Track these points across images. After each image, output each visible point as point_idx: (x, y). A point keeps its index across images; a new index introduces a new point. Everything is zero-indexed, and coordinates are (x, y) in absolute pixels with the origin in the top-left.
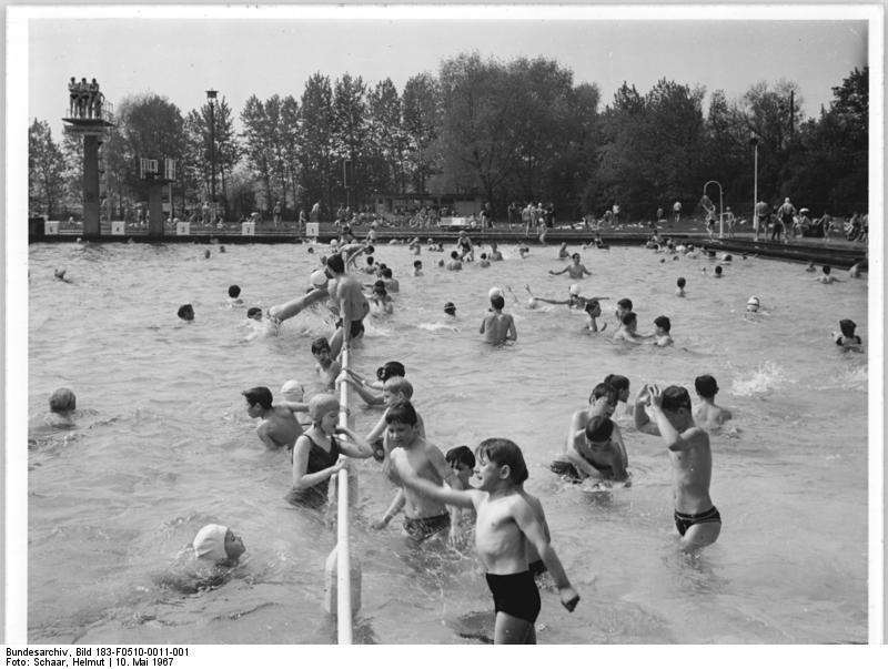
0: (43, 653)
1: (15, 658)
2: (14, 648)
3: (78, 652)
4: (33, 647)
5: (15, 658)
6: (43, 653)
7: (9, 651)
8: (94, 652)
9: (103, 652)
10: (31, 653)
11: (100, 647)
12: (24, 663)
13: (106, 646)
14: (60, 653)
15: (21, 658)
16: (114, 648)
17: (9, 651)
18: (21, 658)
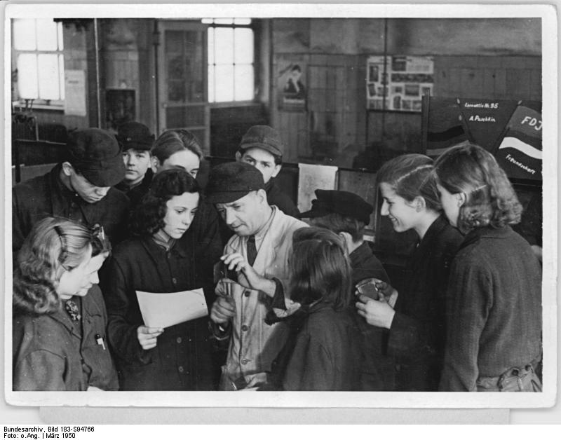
0: (27, 430)
1: (10, 433)
2: (9, 427)
3: (50, 429)
4: (21, 426)
5: (10, 433)
6: (27, 430)
7: (5, 429)
8: (59, 429)
9: (65, 428)
10: (20, 430)
11: (63, 426)
12: (15, 436)
13: (67, 426)
14: (38, 430)
15: (13, 433)
16: (60, 427)
17: (5, 429)
18: (13, 433)
